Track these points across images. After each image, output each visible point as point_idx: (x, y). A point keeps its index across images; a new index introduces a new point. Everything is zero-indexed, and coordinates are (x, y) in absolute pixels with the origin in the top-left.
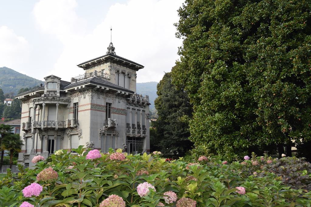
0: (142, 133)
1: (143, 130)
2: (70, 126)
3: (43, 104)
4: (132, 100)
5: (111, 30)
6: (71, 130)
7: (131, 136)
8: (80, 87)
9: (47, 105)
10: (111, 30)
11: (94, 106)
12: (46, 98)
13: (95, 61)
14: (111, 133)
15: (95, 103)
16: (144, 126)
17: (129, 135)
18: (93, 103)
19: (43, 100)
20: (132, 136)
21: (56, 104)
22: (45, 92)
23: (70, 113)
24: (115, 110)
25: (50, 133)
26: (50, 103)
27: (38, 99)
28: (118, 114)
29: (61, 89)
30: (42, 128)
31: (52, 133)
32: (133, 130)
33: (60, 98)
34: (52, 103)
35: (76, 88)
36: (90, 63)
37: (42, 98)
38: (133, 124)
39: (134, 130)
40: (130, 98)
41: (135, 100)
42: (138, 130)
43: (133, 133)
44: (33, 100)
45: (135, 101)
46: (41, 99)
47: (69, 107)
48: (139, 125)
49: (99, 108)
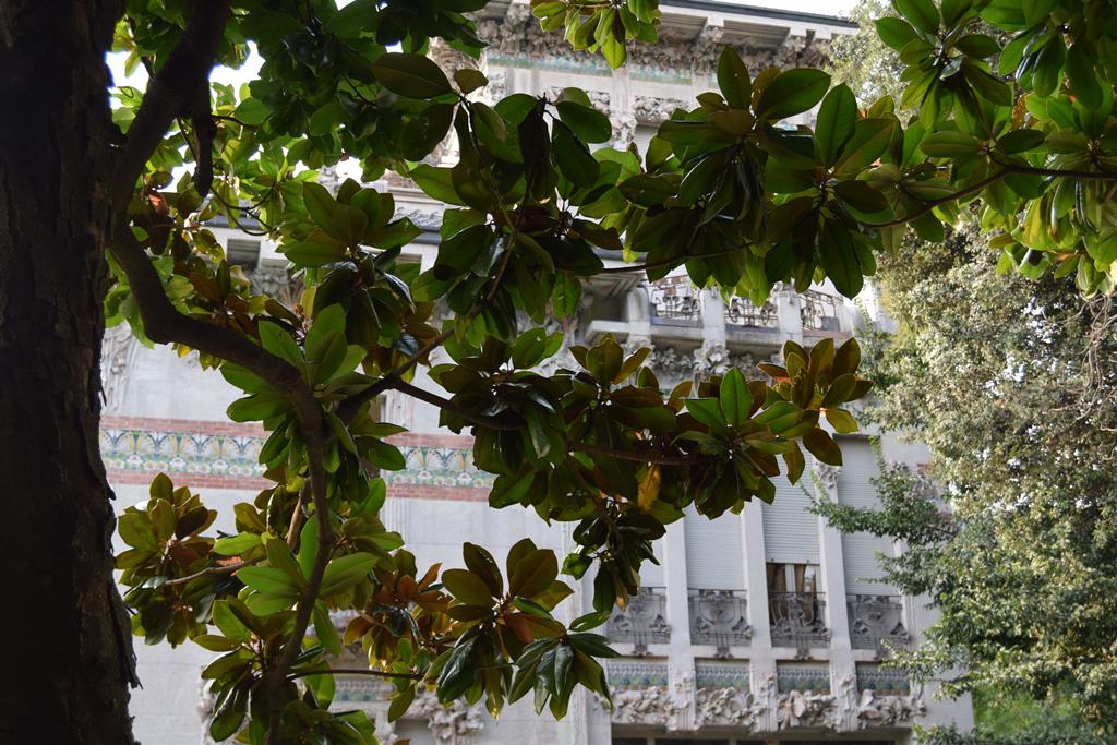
0: (840, 676)
1: (856, 641)
4: (654, 339)
7: (673, 724)
11: (144, 443)
14: (367, 699)
15: (161, 411)
16: (728, 595)
17: (651, 719)
18: (133, 413)
20: (692, 723)
24: (435, 462)
28: (469, 499)
32: (709, 651)
38: (714, 582)
39: (723, 658)
40: (618, 314)
41: (693, 333)
42: (789, 653)
43: (702, 684)
45: (699, 343)
48: (814, 594)
49: (207, 451)
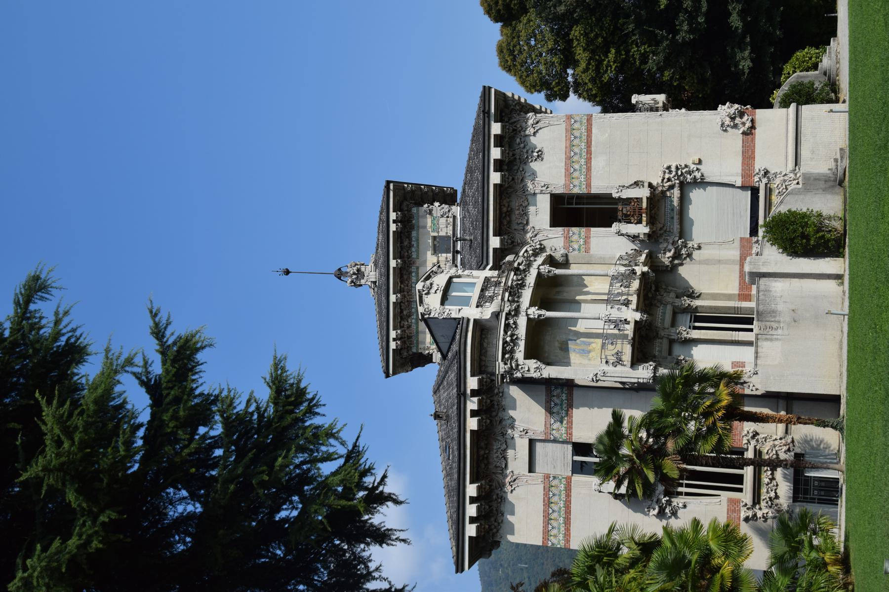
2: (644, 205)
3: (530, 311)
5: (287, 272)
6: (659, 226)
8: (496, 153)
9: (539, 300)
10: (287, 272)
12: (507, 294)
13: (393, 263)
19: (517, 311)
21: (539, 275)
22: (477, 317)
23: (587, 251)
25: (663, 320)
26: (531, 290)
27: (506, 332)
29: (481, 266)
30: (638, 316)
31: (664, 313)
33: (521, 254)
34: (532, 284)
35: (495, 178)
36: (393, 298)
37: (507, 310)
44: (502, 365)
46: (507, 319)
47: (563, 251)
